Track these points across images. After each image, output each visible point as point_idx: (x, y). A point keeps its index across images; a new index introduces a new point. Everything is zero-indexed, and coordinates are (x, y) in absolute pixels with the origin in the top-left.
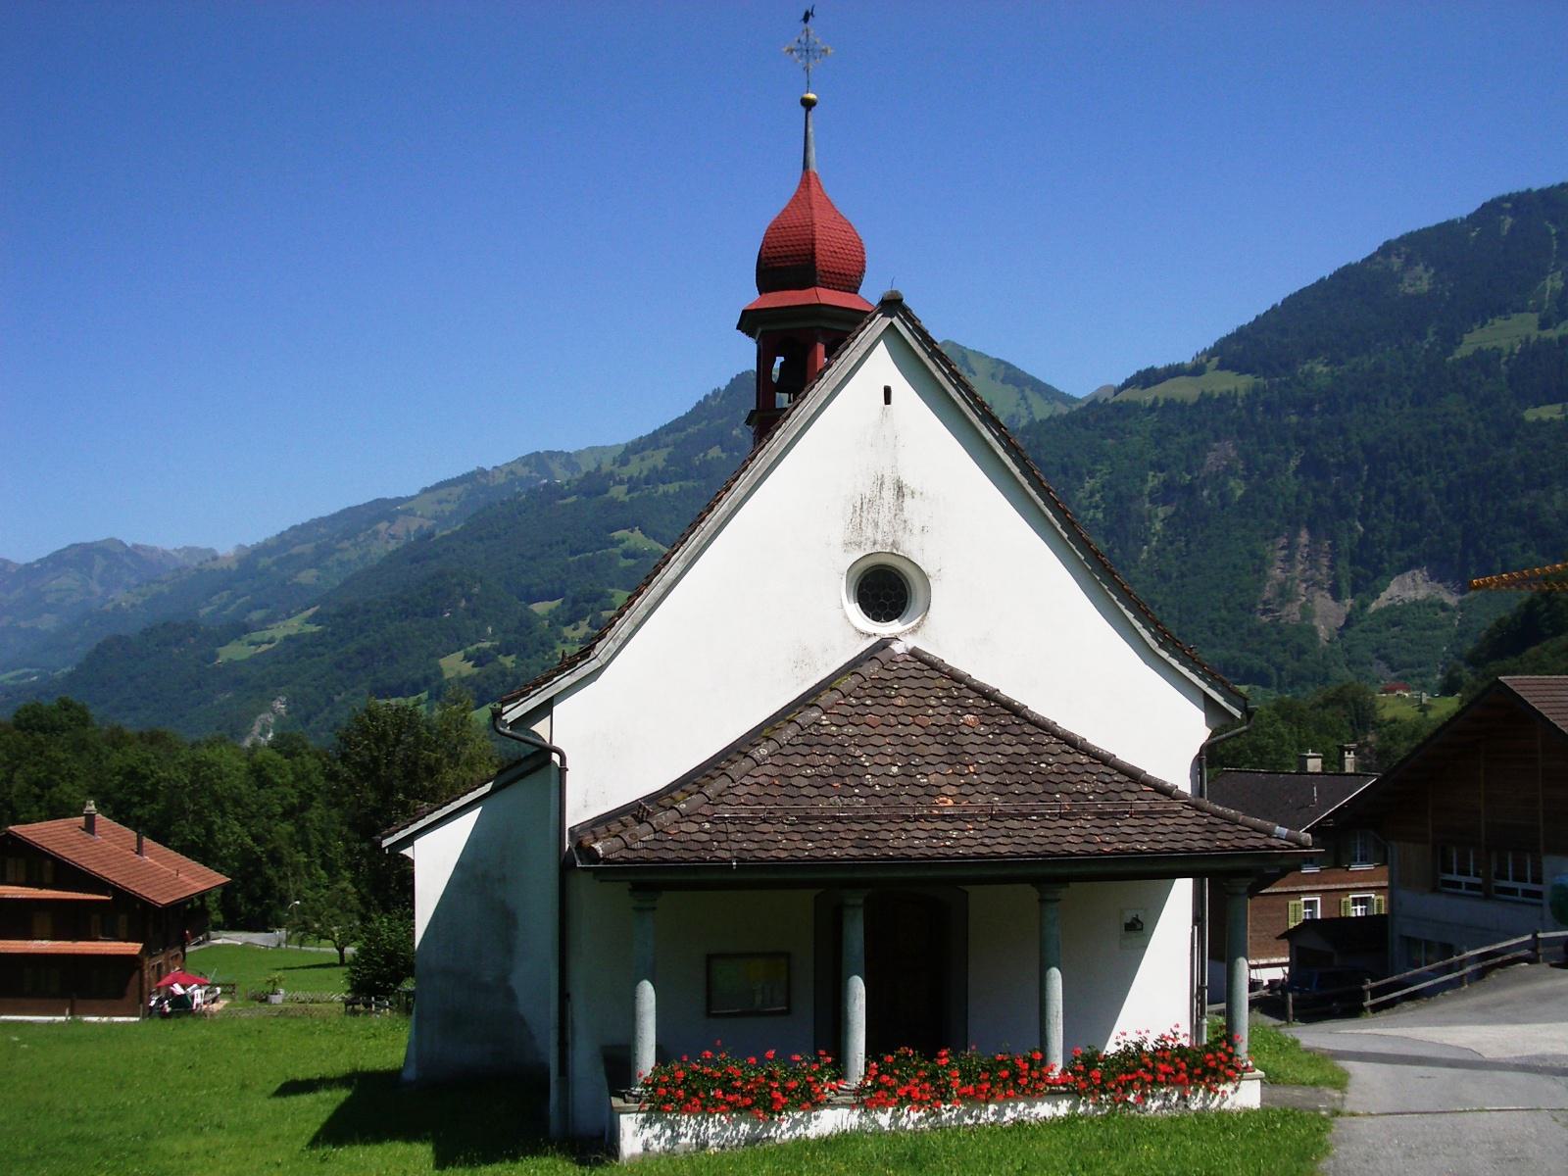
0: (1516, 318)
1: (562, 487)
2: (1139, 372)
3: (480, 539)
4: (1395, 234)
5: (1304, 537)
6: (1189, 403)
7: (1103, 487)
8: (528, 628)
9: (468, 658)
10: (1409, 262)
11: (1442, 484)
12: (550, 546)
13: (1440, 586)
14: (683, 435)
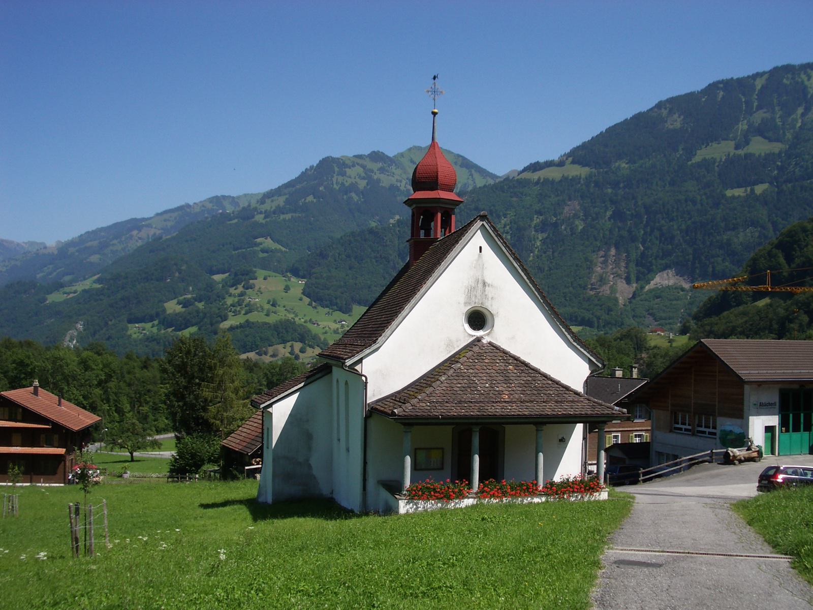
0: (723, 143)
3: (187, 241)
4: (664, 98)
5: (613, 251)
8: (211, 288)
9: (179, 303)
10: (671, 112)
11: (683, 227)
12: (223, 246)
14: (294, 189)
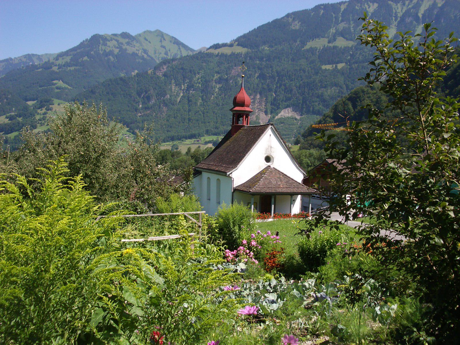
0: (322, 39)
1: (37, 66)
2: (214, 44)
3: (11, 81)
4: (291, 11)
5: (258, 96)
6: (228, 55)
7: (202, 77)
8: (26, 109)
9: (7, 118)
10: (294, 20)
11: (298, 84)
12: (33, 84)
13: (295, 113)
14: (76, 52)
